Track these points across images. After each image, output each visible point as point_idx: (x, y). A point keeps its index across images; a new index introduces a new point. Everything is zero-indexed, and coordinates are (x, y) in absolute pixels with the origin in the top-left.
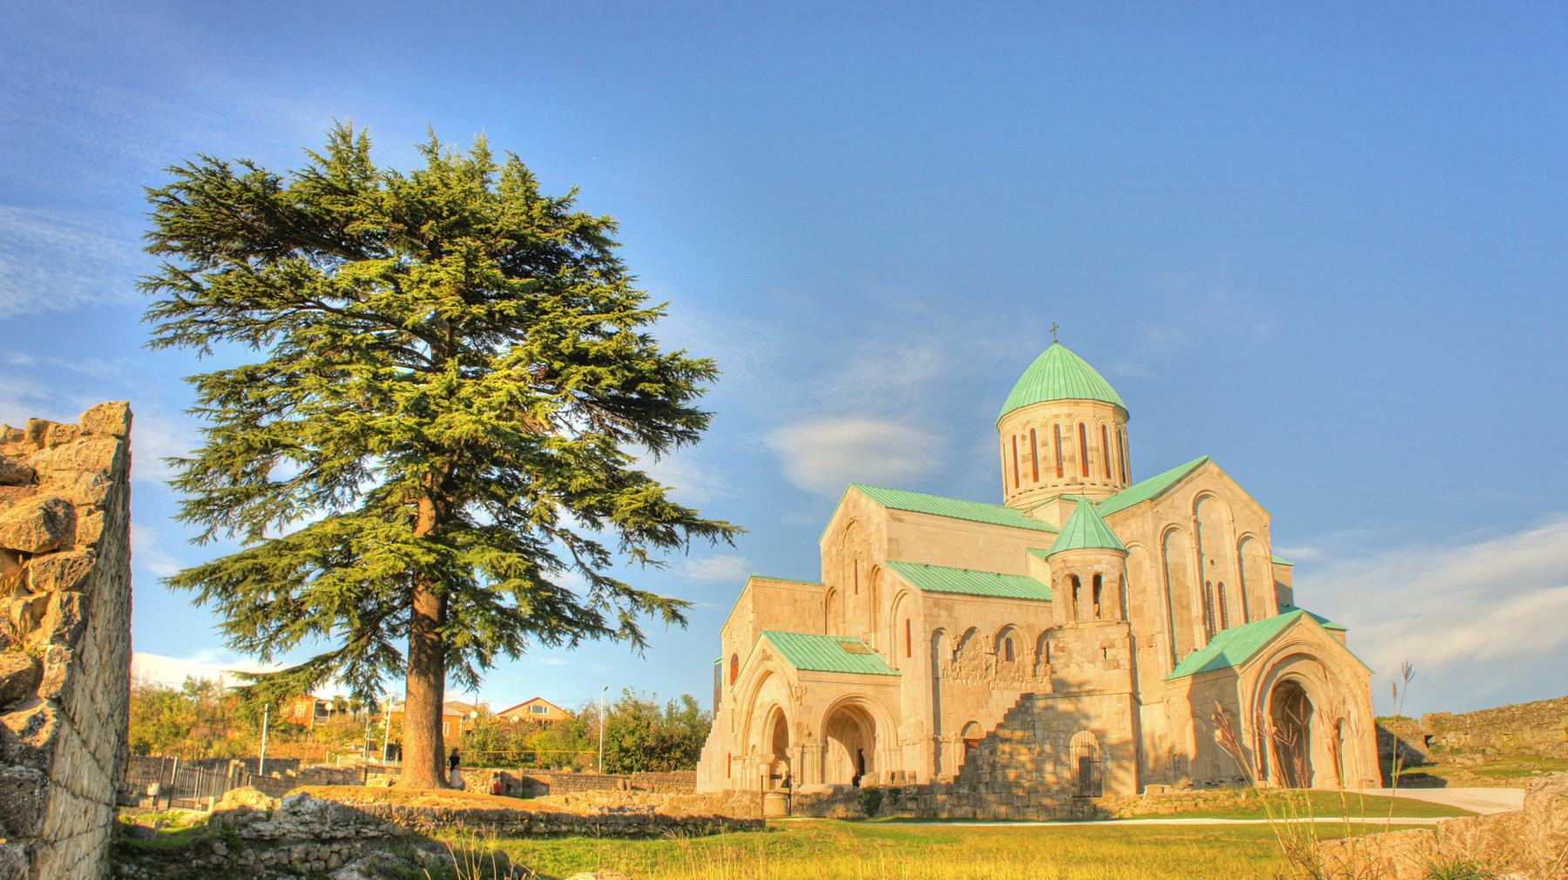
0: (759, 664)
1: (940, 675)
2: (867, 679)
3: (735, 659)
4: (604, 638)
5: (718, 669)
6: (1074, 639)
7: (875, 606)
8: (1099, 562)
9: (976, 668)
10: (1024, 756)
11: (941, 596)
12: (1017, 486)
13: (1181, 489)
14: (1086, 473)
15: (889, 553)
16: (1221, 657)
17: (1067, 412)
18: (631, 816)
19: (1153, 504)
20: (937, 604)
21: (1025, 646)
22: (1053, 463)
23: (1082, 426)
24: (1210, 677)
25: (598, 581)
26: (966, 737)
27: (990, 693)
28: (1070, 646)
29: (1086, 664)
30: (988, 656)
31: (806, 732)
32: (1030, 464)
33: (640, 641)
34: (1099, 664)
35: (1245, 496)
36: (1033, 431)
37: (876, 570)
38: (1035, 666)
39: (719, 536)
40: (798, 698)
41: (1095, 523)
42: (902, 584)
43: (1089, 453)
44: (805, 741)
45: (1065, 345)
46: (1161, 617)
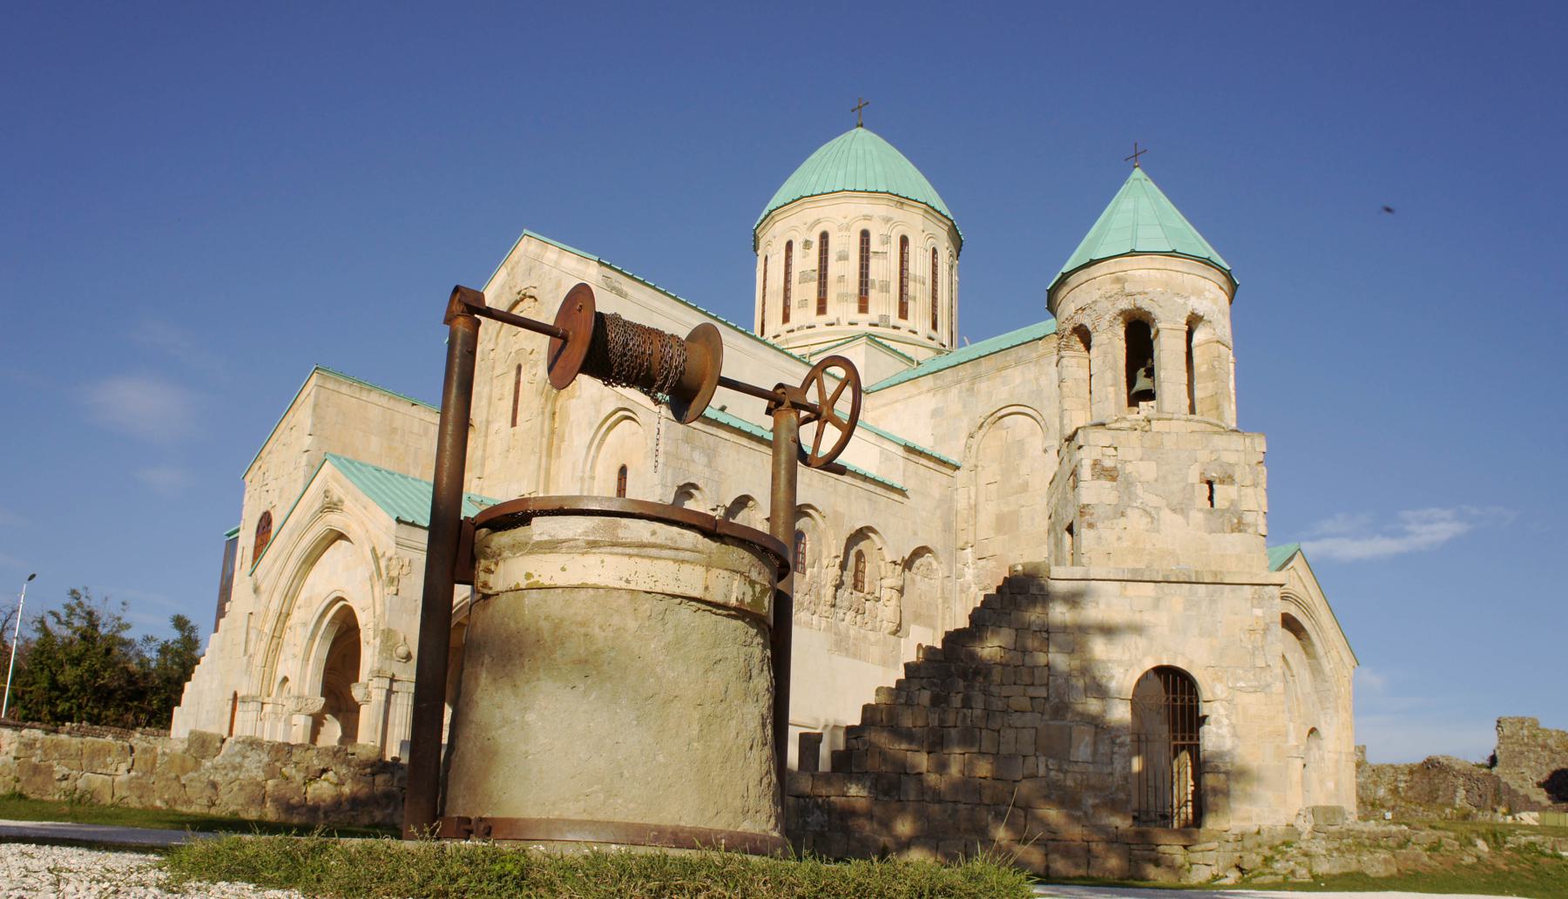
0: (315, 519)
3: (265, 522)
5: (232, 544)
6: (1139, 452)
7: (550, 445)
12: (786, 319)
14: (903, 314)
17: (884, 214)
22: (854, 287)
23: (904, 241)
28: (1129, 468)
29: (1166, 515)
32: (814, 285)
34: (1197, 517)
36: (824, 237)
40: (391, 580)
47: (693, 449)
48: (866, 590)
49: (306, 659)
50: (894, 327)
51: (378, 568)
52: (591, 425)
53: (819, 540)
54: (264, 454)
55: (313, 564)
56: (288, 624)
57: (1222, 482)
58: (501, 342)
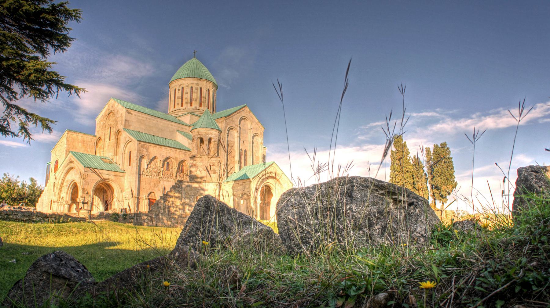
0: (68, 164)
1: (142, 174)
2: (113, 173)
3: (57, 162)
4: (10, 136)
5: (48, 167)
7: (117, 146)
8: (211, 134)
9: (155, 172)
10: (178, 203)
11: (144, 144)
12: (174, 107)
13: (236, 115)
14: (201, 106)
15: (125, 125)
16: (245, 174)
18: (25, 212)
19: (226, 119)
20: (142, 147)
21: (174, 165)
22: (189, 100)
23: (201, 89)
24: (241, 182)
25: (9, 106)
26: (150, 197)
27: (159, 182)
30: (160, 168)
31: (86, 192)
32: (180, 100)
33: (29, 136)
35: (257, 121)
36: (183, 88)
37: (119, 132)
38: (177, 173)
39: (73, 91)
41: (211, 119)
42: (129, 138)
43: (202, 99)
44: (85, 195)
45: (198, 59)
46: (225, 159)
47: (143, 148)
48: (184, 173)
49: (67, 193)
50: (198, 109)
51: (81, 176)
52: (124, 143)
53: (173, 163)
54: (56, 147)
55: (68, 173)
56: (63, 186)
57: (212, 166)
58: (107, 121)
